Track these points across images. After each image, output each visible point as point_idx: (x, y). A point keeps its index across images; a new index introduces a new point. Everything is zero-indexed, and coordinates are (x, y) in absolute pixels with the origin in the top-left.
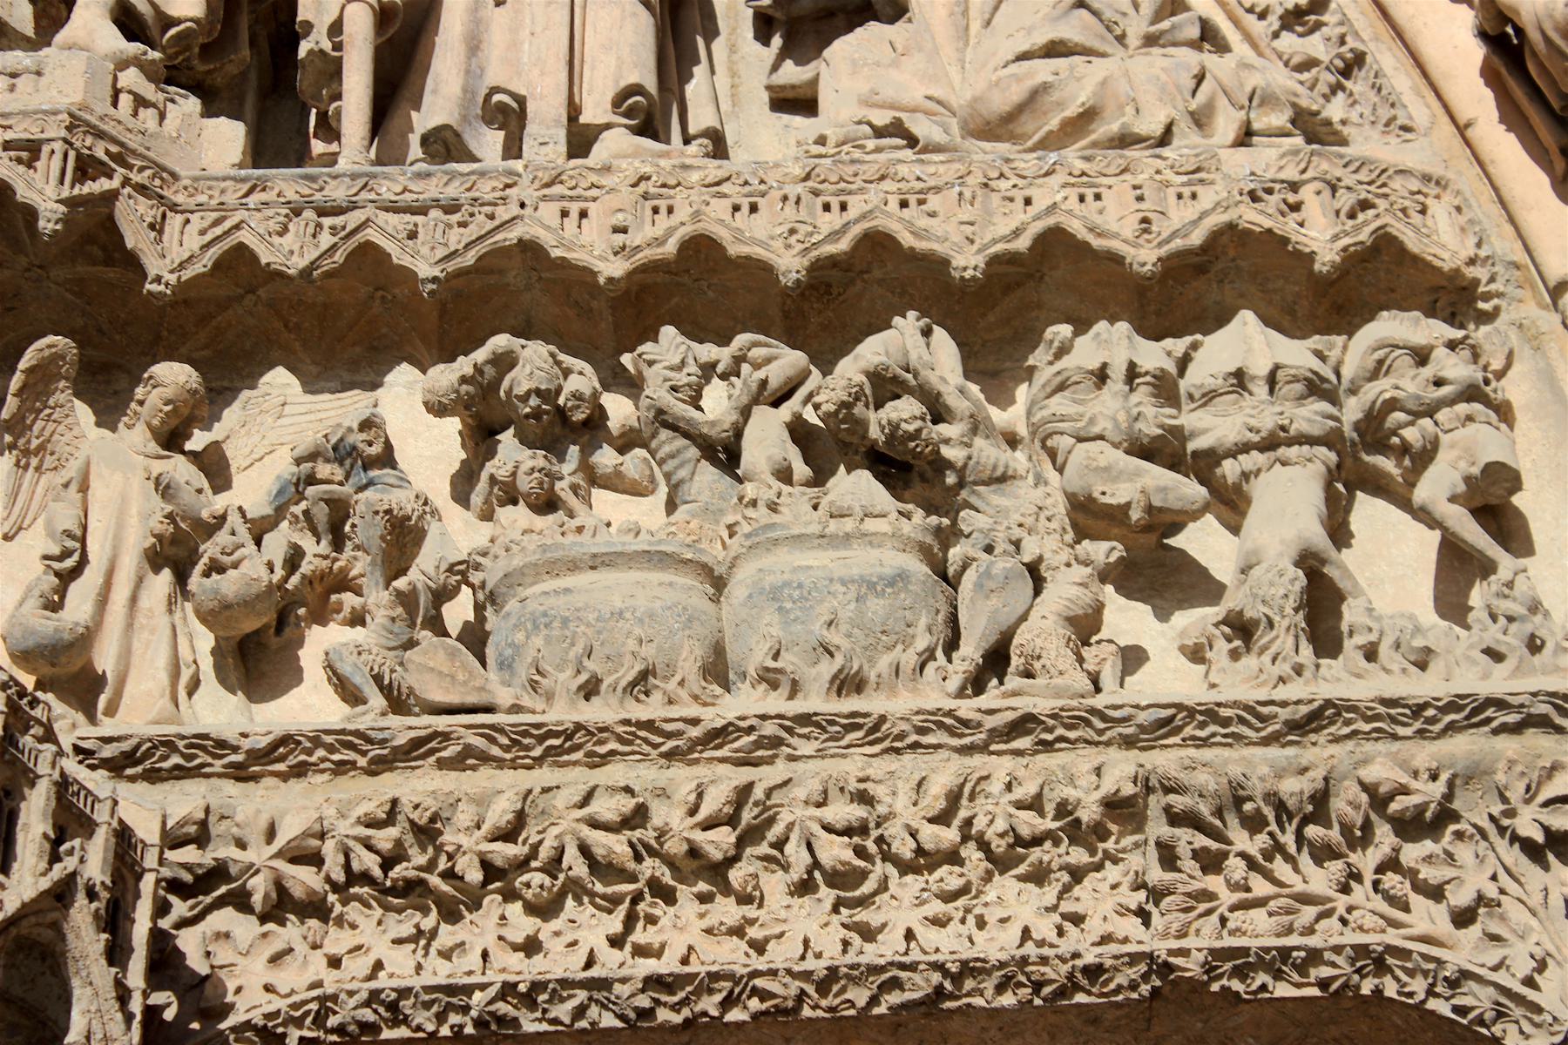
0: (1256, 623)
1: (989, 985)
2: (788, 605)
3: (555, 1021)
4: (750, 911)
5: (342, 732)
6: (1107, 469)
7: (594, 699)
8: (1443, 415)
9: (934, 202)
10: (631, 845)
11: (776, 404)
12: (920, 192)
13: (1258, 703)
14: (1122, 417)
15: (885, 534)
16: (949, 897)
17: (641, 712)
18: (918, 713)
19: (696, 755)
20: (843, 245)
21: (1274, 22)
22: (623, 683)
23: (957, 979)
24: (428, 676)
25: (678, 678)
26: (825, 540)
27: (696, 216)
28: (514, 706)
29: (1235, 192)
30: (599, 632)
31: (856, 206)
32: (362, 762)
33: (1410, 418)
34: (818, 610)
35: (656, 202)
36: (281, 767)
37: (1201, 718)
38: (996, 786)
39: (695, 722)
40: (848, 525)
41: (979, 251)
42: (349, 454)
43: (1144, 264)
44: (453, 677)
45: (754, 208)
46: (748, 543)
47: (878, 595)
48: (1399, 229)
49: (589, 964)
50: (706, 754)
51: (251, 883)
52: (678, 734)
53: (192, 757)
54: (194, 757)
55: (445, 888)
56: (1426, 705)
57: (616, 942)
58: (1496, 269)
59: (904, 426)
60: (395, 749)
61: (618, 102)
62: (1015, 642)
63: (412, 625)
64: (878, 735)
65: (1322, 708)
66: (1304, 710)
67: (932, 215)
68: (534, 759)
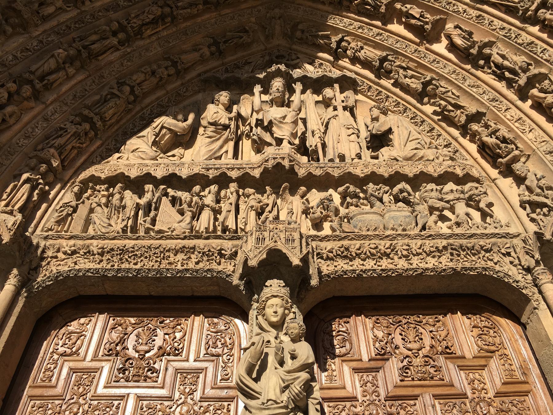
1: (429, 272)
8: (481, 196)
16: (422, 259)
17: (375, 233)
20: (393, 173)
21: (443, 146)
23: (425, 270)
31: (394, 168)
38: (427, 244)
40: (401, 209)
48: (469, 172)
49: (372, 267)
57: (375, 264)
61: (356, 155)
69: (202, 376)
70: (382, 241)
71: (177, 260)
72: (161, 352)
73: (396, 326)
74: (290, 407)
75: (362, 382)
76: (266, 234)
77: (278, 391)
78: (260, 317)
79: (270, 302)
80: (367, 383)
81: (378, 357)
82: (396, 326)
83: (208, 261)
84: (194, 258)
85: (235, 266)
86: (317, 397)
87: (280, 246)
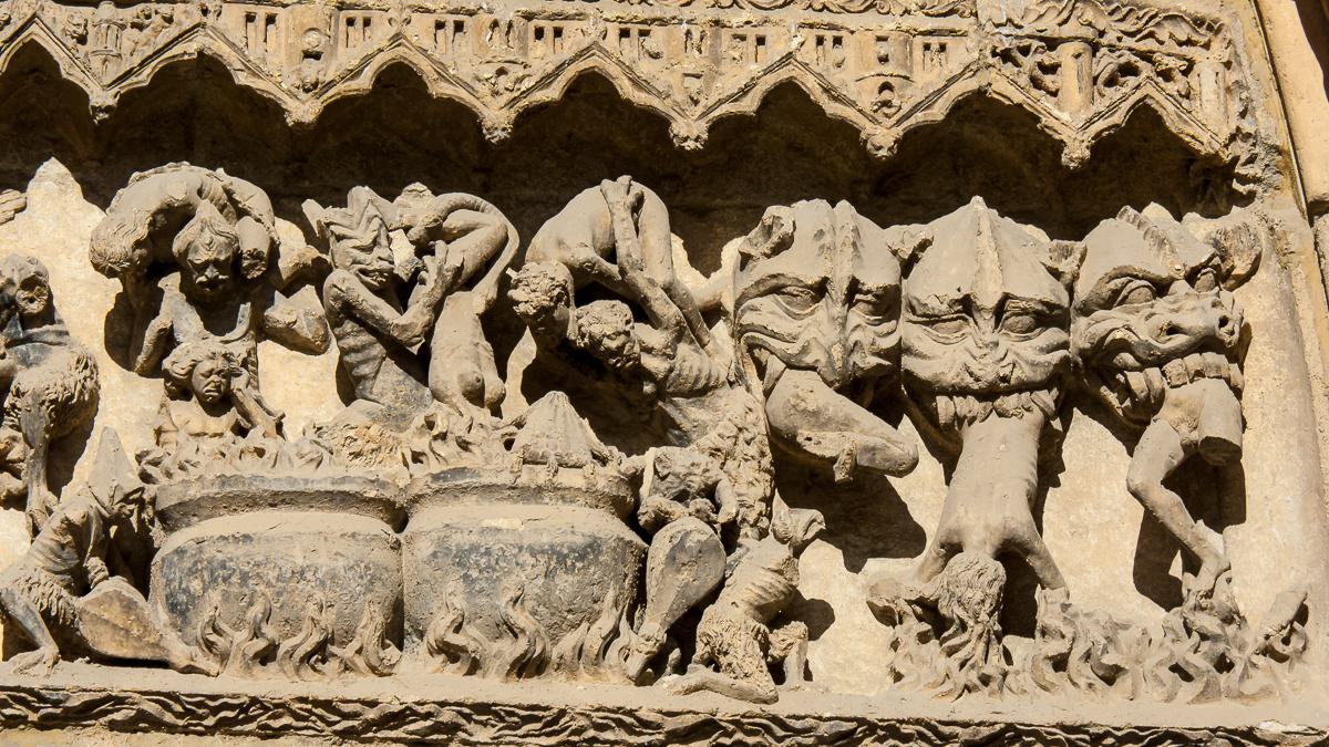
0: (952, 621)
2: (474, 574)
5: (18, 689)
6: (815, 414)
7: (272, 666)
8: (1173, 367)
9: (658, 36)
11: (470, 283)
12: (644, 22)
13: (939, 722)
14: (837, 352)
15: (579, 489)
18: (598, 710)
19: (370, 734)
22: (301, 652)
24: (102, 628)
25: (355, 645)
26: (516, 492)
27: (397, 39)
28: (187, 667)
29: (988, 52)
30: (279, 594)
31: (573, 39)
32: (33, 717)
33: (1138, 364)
34: (505, 582)
35: (352, 13)
37: (882, 733)
39: (373, 704)
40: (541, 475)
41: (704, 115)
42: (7, 306)
43: (880, 148)
44: (127, 631)
45: (459, 27)
46: (435, 486)
47: (570, 570)
50: (379, 735)
52: (354, 715)
56: (1107, 734)
58: (1257, 150)
59: (606, 342)
60: (67, 710)
62: (701, 628)
63: (82, 555)
64: (556, 727)
65: (1003, 731)
66: (985, 731)
67: (656, 56)
68: (206, 727)
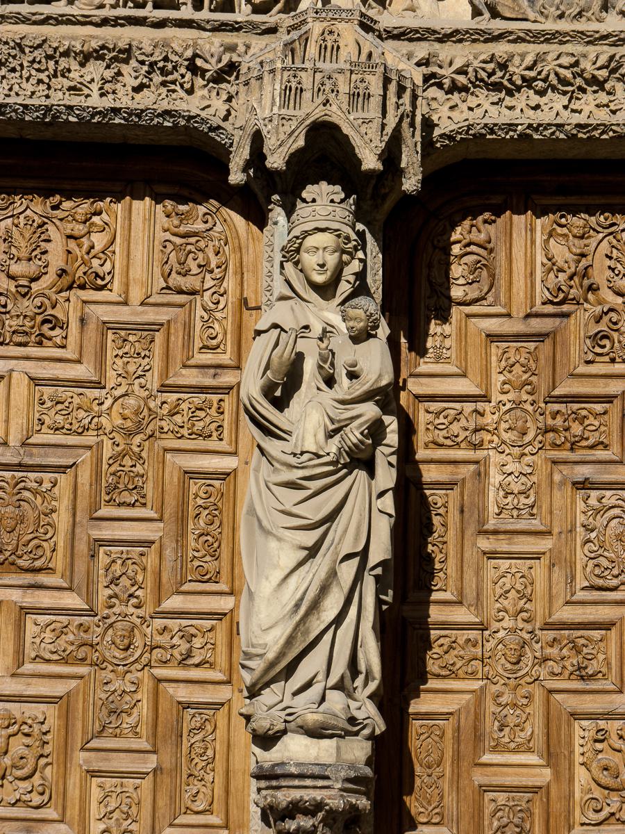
3: (545, 136)
4: (612, 98)
5: (477, 29)
7: (563, 20)
10: (573, 73)
22: (573, 15)
24: (505, 8)
32: (482, 39)
36: (454, 39)
39: (597, 32)
51: (444, 81)
53: (425, 34)
54: (425, 34)
55: (509, 86)
57: (566, 107)
60: (493, 36)
69: (159, 337)
70: (590, 48)
71: (88, 78)
72: (66, 280)
73: (601, 235)
74: (342, 462)
75: (503, 363)
76: (306, 79)
77: (321, 436)
78: (289, 266)
79: (310, 241)
80: (512, 366)
81: (550, 309)
82: (601, 235)
83: (164, 84)
84: (130, 74)
85: (229, 99)
86: (392, 444)
87: (337, 114)
